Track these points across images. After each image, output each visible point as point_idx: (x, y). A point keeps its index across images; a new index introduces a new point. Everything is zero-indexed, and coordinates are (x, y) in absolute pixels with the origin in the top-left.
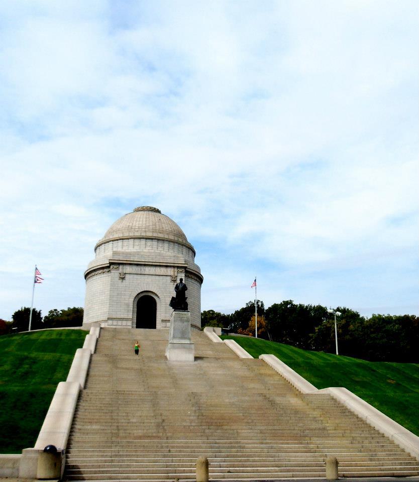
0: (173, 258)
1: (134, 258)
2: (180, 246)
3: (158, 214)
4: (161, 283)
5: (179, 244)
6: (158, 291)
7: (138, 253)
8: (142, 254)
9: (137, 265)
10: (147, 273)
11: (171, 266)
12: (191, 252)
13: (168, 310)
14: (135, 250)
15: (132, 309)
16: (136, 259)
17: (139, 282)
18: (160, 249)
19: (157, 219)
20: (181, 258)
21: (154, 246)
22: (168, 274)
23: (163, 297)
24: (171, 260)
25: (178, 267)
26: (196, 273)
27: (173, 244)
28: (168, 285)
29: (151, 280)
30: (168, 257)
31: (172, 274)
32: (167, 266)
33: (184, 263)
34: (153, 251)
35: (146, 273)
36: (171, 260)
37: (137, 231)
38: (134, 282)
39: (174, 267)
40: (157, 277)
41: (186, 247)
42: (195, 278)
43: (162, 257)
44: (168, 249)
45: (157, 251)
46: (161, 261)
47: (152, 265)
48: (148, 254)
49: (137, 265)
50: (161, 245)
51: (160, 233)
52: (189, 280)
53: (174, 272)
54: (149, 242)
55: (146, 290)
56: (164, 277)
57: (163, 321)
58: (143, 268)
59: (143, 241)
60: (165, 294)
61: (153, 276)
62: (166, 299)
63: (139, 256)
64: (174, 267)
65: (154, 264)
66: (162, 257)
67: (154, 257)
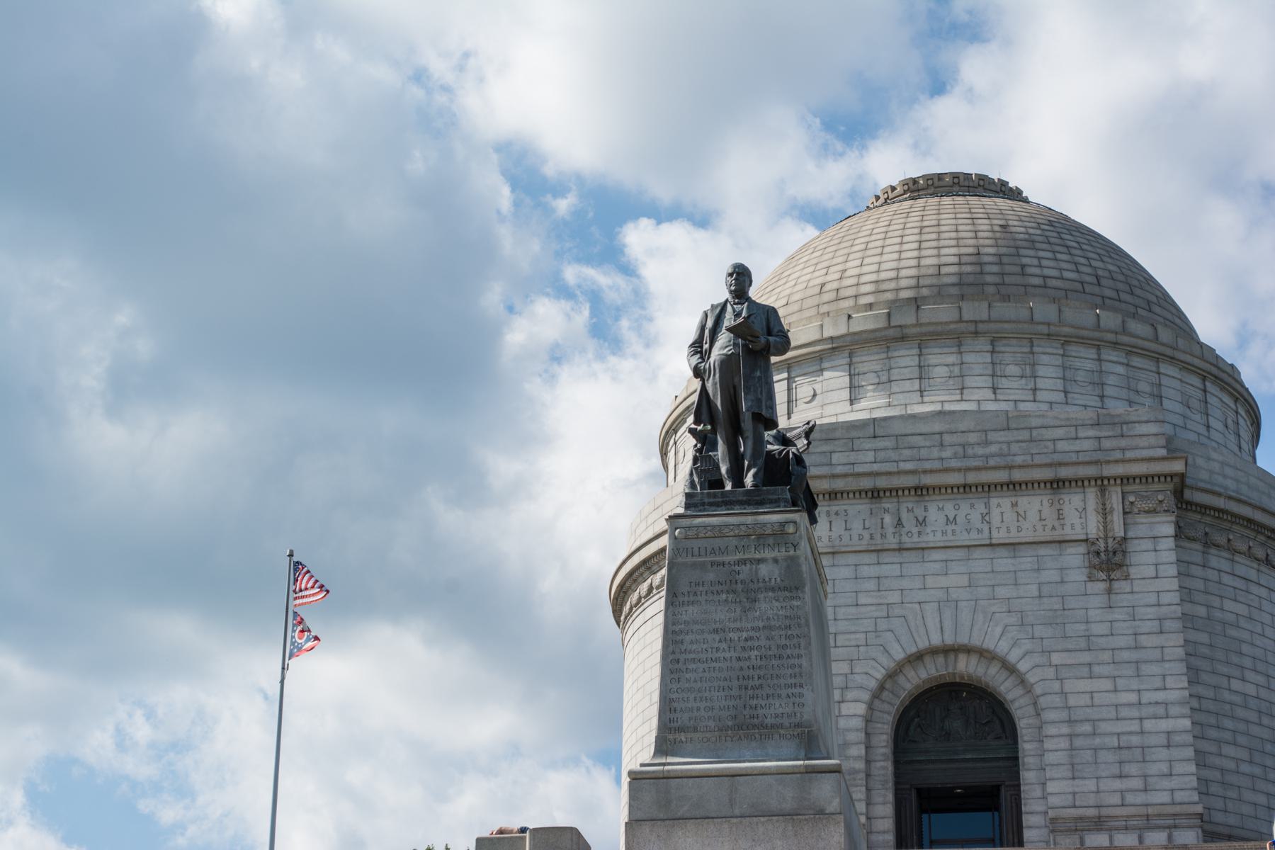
0: (1091, 433)
1: (853, 457)
2: (1137, 361)
3: (1003, 203)
4: (1033, 590)
5: (1131, 351)
6: (1015, 644)
7: (872, 428)
8: (898, 428)
9: (875, 494)
10: (938, 539)
11: (1080, 483)
12: (1217, 398)
13: (1088, 755)
14: (864, 416)
15: (860, 765)
16: (865, 460)
17: (894, 597)
18: (1014, 388)
19: (983, 225)
20: (1144, 429)
21: (969, 382)
22: (1068, 533)
23: (1050, 673)
24: (1078, 446)
25: (1126, 480)
26: (1259, 517)
27: (1092, 353)
28: (1071, 603)
29: (964, 580)
30: (1060, 433)
31: (1093, 527)
32: (1057, 485)
33: (1163, 452)
34: (971, 406)
35: (931, 538)
36: (1078, 446)
37: (870, 306)
38: (863, 599)
39: (1102, 483)
40: (1004, 562)
41: (1187, 367)
42: (1260, 553)
43: (1025, 435)
44: (1059, 384)
45: (992, 406)
46: (1019, 460)
47: (966, 488)
48: (937, 427)
49: (875, 494)
50: (1013, 370)
51: (1006, 298)
52: (1218, 560)
53: (1105, 512)
54: (941, 360)
55: (936, 640)
56: (1043, 551)
57: (1055, 826)
58: (908, 509)
59: (906, 359)
60: (1056, 658)
61: (977, 553)
62: (1069, 686)
63: (880, 443)
64: (1102, 483)
65: (972, 478)
66: (1025, 435)
67: (973, 438)
